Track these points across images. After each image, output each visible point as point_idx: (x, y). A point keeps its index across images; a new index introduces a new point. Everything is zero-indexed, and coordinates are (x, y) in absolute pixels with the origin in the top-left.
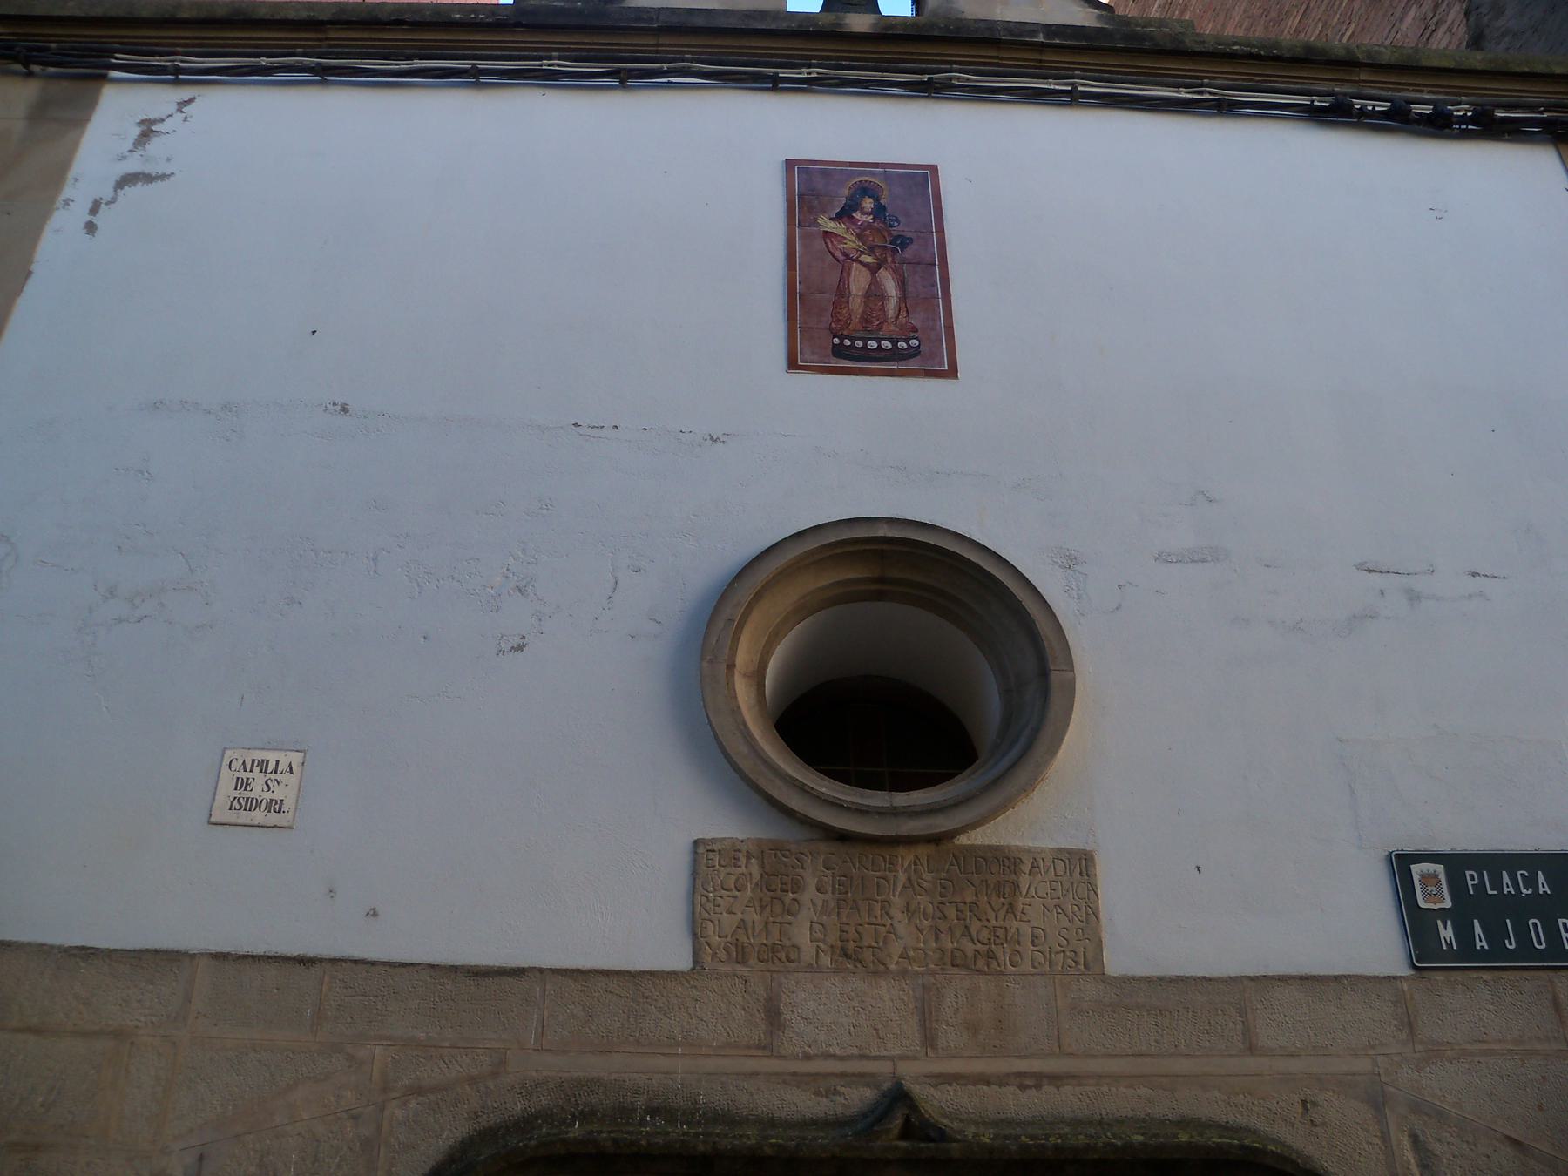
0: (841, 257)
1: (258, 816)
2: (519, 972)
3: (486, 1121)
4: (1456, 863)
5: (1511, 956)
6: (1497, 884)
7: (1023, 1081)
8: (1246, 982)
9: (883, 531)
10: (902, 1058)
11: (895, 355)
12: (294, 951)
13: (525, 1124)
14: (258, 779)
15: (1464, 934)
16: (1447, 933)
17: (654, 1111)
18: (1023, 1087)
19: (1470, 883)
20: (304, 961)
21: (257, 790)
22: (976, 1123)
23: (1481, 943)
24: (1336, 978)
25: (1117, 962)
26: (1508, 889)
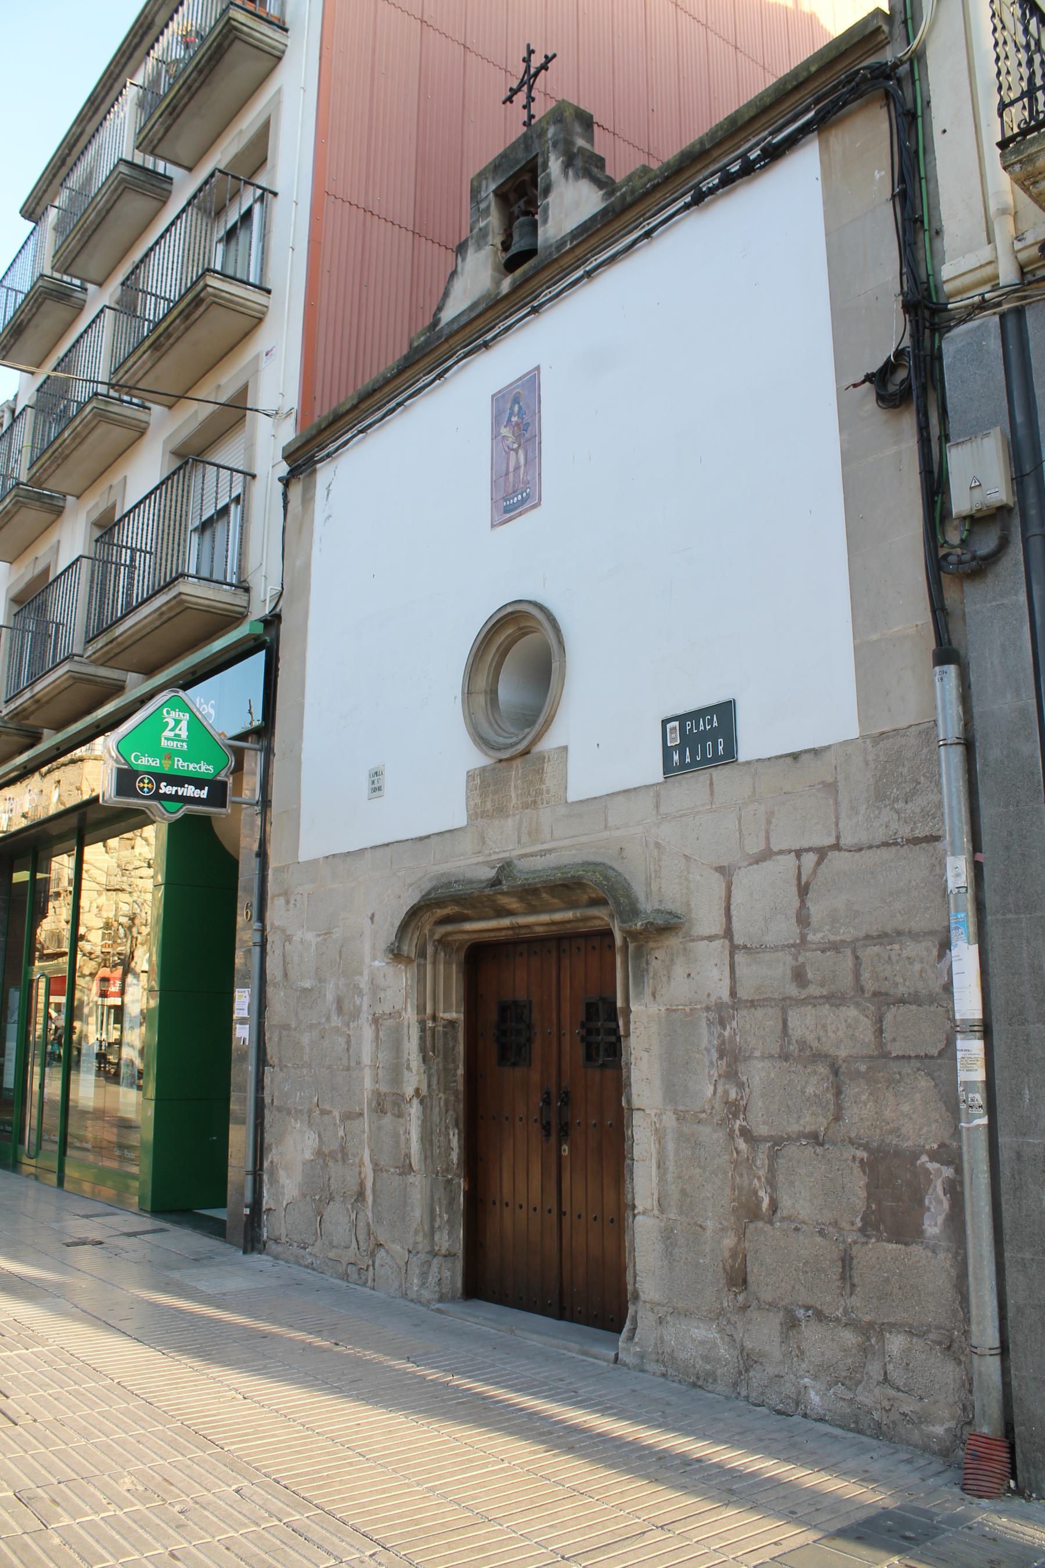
0: (507, 449)
1: (377, 793)
2: (428, 837)
3: (423, 893)
4: (682, 718)
5: (699, 764)
6: (697, 727)
7: (543, 853)
8: (607, 798)
9: (509, 609)
10: (513, 850)
11: (523, 502)
12: (386, 842)
13: (429, 893)
14: (376, 778)
15: (682, 756)
16: (676, 757)
17: (456, 882)
18: (541, 856)
19: (688, 728)
20: (388, 845)
21: (376, 785)
22: (527, 873)
23: (688, 760)
24: (635, 789)
25: (572, 797)
26: (702, 728)
